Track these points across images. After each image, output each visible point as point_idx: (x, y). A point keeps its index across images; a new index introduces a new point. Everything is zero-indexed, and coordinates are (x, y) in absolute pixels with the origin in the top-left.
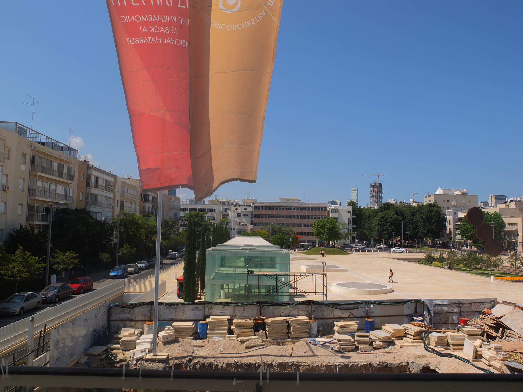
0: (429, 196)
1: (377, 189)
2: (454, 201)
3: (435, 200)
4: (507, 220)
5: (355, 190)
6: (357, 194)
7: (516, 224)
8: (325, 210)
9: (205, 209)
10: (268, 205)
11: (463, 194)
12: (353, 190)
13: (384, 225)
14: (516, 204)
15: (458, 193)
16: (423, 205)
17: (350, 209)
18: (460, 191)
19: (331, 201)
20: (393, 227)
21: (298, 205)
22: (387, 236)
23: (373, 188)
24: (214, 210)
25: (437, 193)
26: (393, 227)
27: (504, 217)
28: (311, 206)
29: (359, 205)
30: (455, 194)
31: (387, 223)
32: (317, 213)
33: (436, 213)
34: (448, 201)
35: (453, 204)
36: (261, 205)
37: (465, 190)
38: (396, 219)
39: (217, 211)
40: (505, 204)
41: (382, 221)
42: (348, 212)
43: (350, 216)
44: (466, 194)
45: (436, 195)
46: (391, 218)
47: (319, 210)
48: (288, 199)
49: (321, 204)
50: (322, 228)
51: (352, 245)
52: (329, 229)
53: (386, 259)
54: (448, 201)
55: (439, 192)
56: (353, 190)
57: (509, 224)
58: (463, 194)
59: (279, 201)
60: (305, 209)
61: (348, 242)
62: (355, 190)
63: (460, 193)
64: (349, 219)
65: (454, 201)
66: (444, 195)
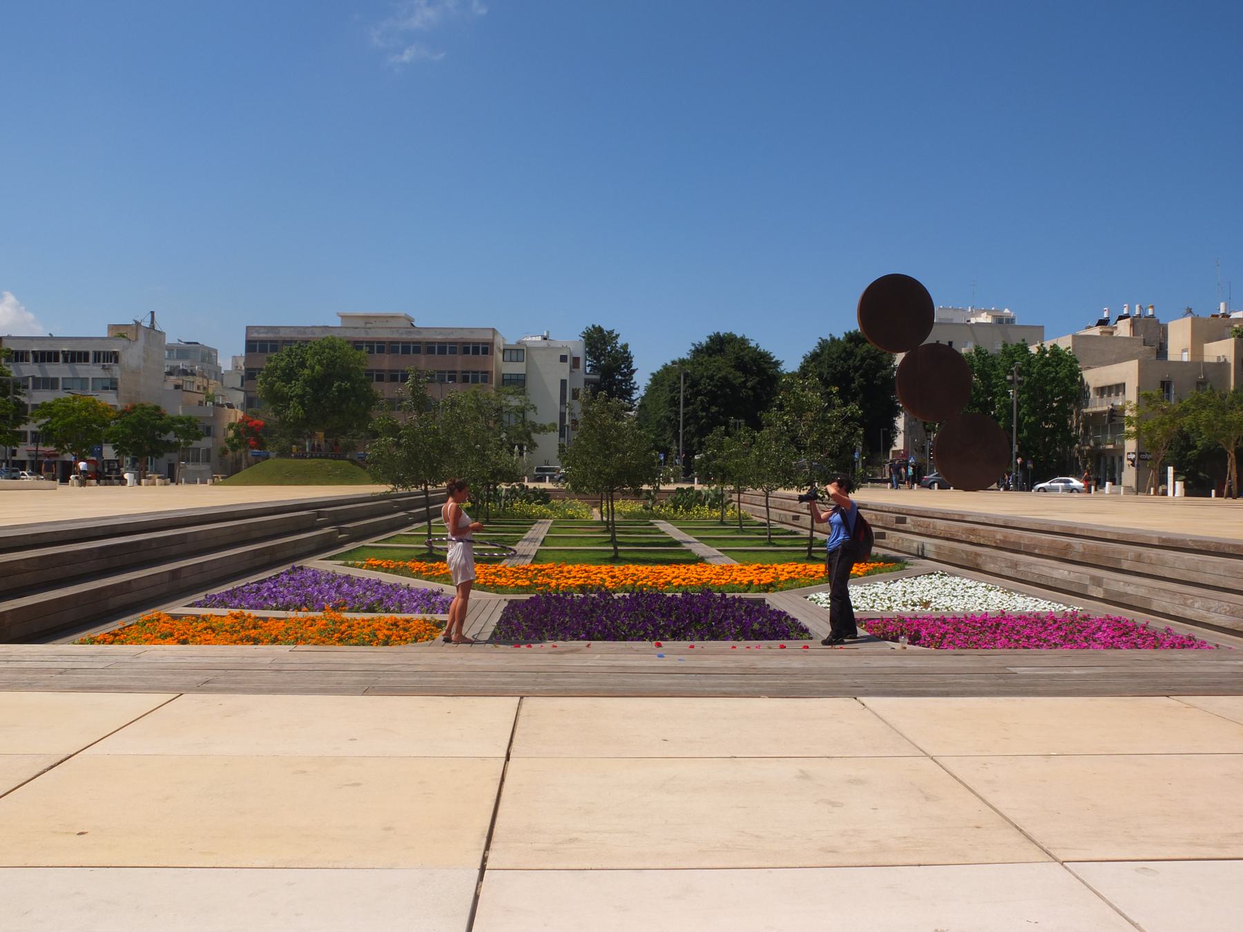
4: (1094, 377)
7: (1119, 388)
8: (485, 351)
9: (87, 354)
10: (294, 335)
11: (1000, 321)
14: (1133, 325)
15: (985, 318)
18: (989, 312)
20: (714, 409)
21: (395, 336)
24: (113, 357)
26: (714, 409)
28: (439, 337)
29: (621, 342)
30: (973, 321)
31: (698, 393)
32: (460, 363)
33: (863, 359)
36: (271, 336)
37: (1007, 311)
38: (725, 382)
39: (124, 359)
44: (1010, 321)
46: (711, 378)
47: (466, 351)
48: (367, 318)
49: (471, 330)
50: (289, 375)
52: (309, 382)
57: (1102, 391)
58: (1000, 321)
59: (337, 322)
60: (417, 350)
63: (989, 320)
64: (563, 382)
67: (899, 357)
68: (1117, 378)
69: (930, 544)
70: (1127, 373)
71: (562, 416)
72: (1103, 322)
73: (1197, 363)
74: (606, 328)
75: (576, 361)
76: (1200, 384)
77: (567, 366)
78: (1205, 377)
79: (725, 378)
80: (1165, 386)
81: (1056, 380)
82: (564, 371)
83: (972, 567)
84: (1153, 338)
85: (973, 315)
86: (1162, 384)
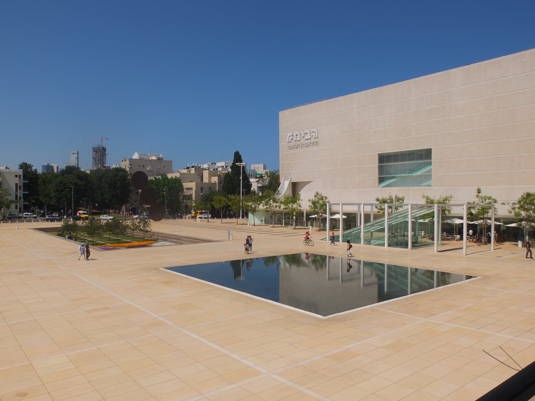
0: (125, 160)
1: (100, 153)
2: (150, 167)
3: (131, 165)
4: (186, 185)
5: (75, 154)
6: (78, 158)
7: (191, 189)
11: (159, 159)
12: (73, 154)
13: (62, 191)
15: (154, 158)
16: (110, 170)
17: (21, 172)
18: (155, 155)
19: (46, 164)
22: (66, 203)
23: (96, 152)
25: (134, 157)
27: (184, 182)
29: (33, 169)
31: (67, 188)
33: (120, 177)
34: (144, 166)
35: (148, 169)
37: (161, 155)
40: (187, 170)
41: (60, 187)
42: (16, 176)
43: (20, 182)
44: (162, 159)
45: (131, 160)
51: (21, 215)
53: (32, 231)
54: (144, 166)
55: (136, 156)
56: (73, 154)
57: (187, 189)
58: (159, 159)
61: (16, 212)
62: (75, 154)
63: (156, 159)
64: (17, 184)
65: (150, 167)
66: (141, 159)
67: (140, 191)
68: (190, 187)
69: (160, 238)
70: (193, 185)
71: (16, 196)
72: (188, 168)
73: (210, 183)
74: (28, 163)
75: (20, 176)
76: (210, 188)
77: (18, 178)
78: (211, 186)
79: (75, 183)
80: (202, 189)
81: (176, 185)
82: (17, 180)
83: (166, 240)
84: (199, 171)
85: (150, 156)
86: (201, 188)
